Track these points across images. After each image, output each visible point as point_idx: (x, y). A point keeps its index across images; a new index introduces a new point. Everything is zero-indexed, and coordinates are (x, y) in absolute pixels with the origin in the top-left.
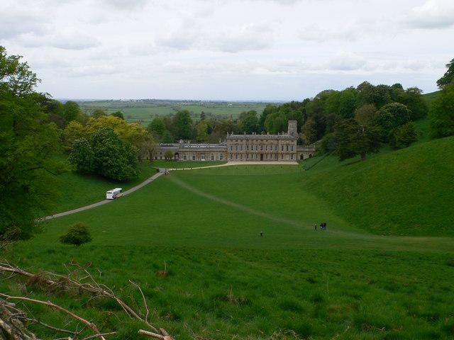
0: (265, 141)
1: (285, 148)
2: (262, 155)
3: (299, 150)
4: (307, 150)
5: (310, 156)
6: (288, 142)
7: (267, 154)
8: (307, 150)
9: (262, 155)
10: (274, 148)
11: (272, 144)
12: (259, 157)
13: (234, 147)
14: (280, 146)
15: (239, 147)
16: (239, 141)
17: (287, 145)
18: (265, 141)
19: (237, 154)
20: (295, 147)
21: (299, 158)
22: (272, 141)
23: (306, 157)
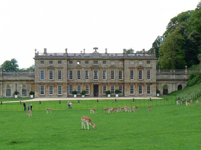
0: (100, 62)
1: (136, 73)
2: (96, 87)
3: (160, 77)
4: (174, 77)
5: (180, 87)
6: (141, 63)
7: (105, 85)
8: (174, 77)
9: (96, 87)
10: (116, 75)
11: (113, 67)
12: (91, 91)
13: (47, 73)
14: (127, 71)
15: (55, 72)
16: (55, 63)
17: (140, 68)
18: (100, 62)
19: (52, 85)
20: (153, 72)
21: (162, 91)
22: (113, 63)
23: (172, 88)
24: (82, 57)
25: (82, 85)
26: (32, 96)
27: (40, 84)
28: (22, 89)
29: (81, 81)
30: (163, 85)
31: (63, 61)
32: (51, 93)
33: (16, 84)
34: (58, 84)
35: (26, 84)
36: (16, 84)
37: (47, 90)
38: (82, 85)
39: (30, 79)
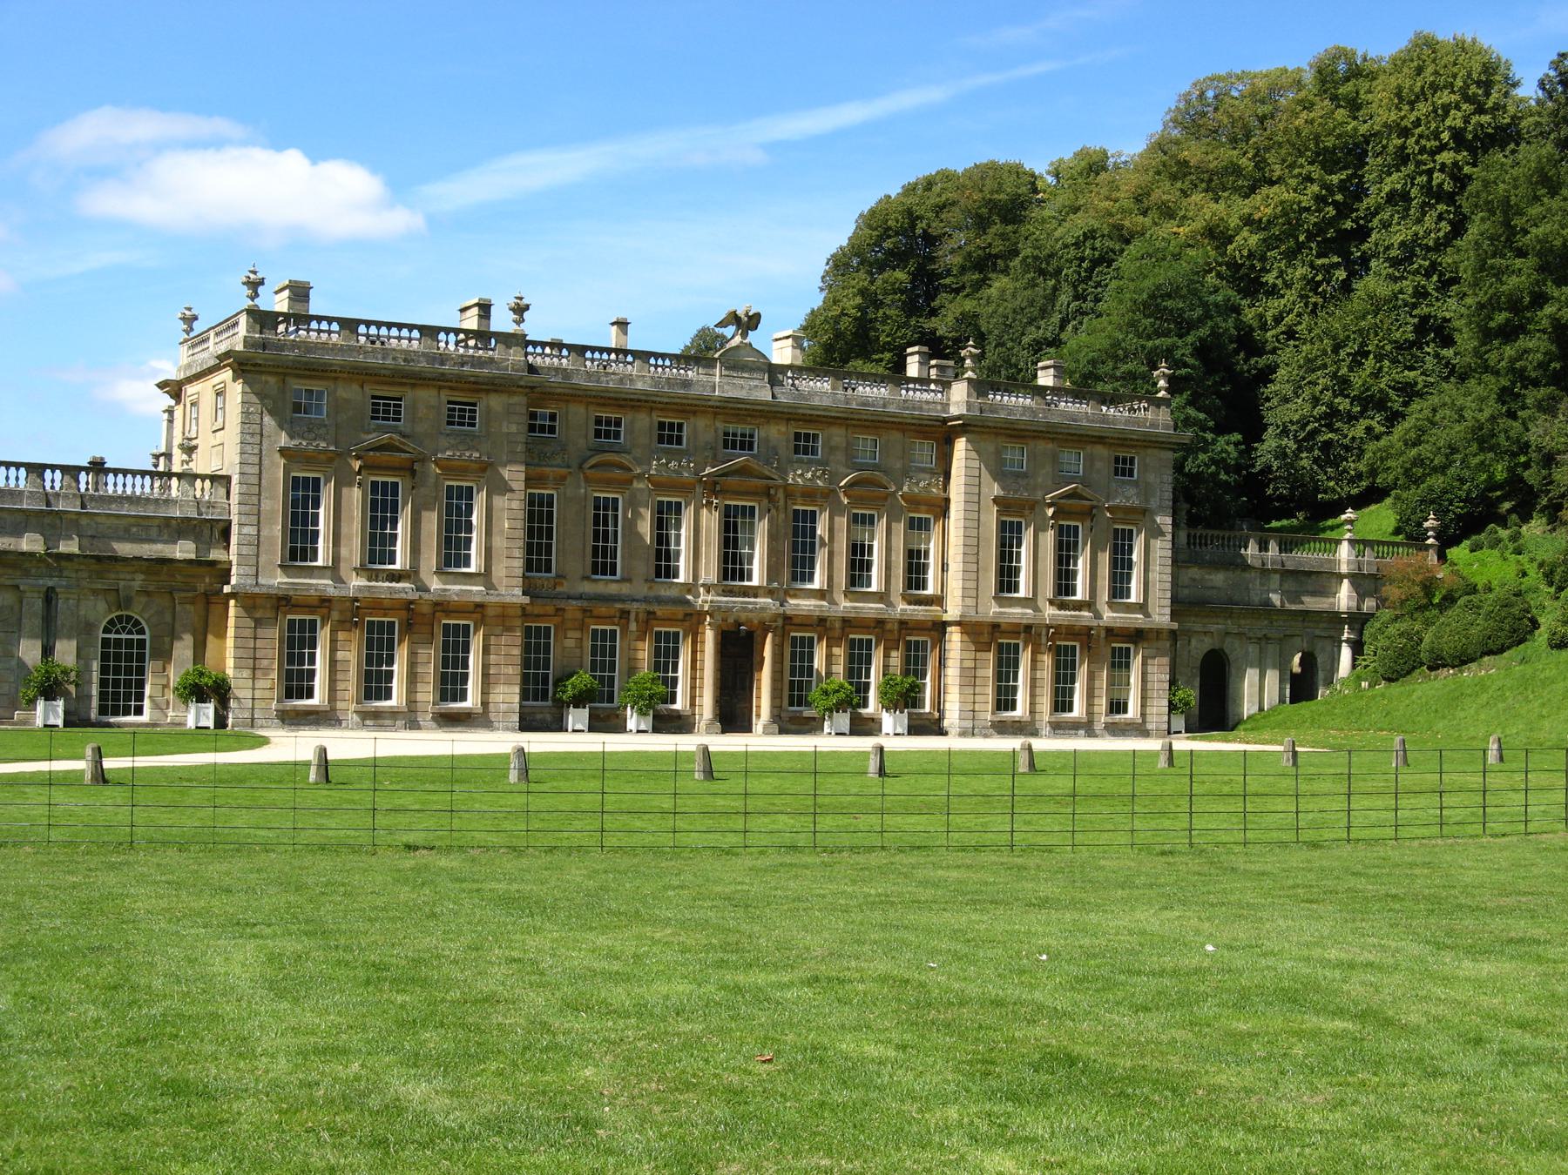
24: (639, 386)
25: (633, 626)
26: (205, 714)
27: (282, 601)
28: (106, 643)
29: (625, 589)
30: (1199, 647)
31: (496, 402)
32: (375, 685)
33: (49, 597)
34: (442, 607)
35: (143, 599)
36: (49, 597)
37: (333, 660)
38: (633, 626)
39: (183, 550)
